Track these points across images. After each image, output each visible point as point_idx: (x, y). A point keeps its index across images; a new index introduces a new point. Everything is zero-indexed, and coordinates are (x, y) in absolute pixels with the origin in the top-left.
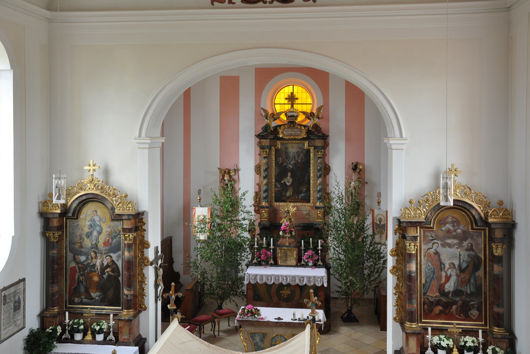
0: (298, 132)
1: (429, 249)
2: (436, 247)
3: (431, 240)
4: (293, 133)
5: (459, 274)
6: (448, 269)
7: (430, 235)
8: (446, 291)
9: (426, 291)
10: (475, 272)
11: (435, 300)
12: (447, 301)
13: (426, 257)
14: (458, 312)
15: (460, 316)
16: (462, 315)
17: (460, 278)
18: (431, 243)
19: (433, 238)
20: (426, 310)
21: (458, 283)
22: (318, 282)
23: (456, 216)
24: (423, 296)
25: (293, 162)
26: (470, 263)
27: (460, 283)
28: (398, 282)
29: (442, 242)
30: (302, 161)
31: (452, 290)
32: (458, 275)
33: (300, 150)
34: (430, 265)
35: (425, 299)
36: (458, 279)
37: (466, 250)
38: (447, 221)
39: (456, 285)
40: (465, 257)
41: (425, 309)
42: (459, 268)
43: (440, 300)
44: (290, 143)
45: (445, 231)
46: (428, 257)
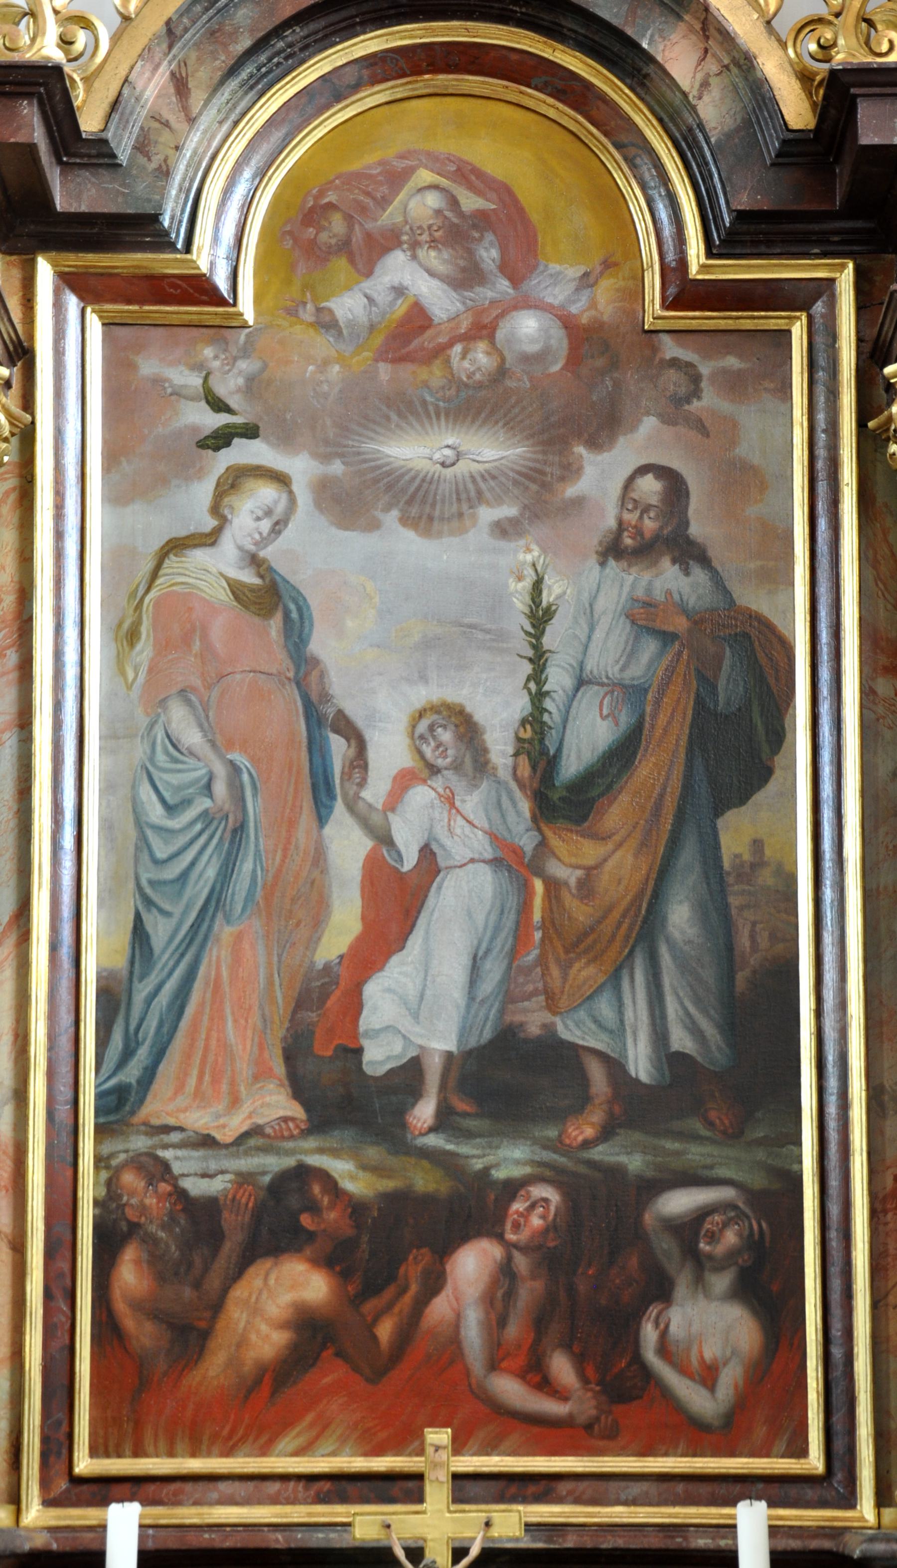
2: (266, 525)
3: (202, 444)
5: (527, 842)
9: (132, 1073)
10: (719, 810)
11: (244, 1179)
12: (388, 1185)
13: (144, 651)
14: (513, 1331)
17: (539, 886)
18: (200, 474)
19: (223, 419)
20: (129, 1322)
21: (514, 954)
24: (101, 1130)
26: (657, 703)
27: (541, 960)
29: (326, 458)
32: (517, 852)
34: (192, 737)
35: (129, 1178)
36: (512, 902)
38: (390, 216)
39: (488, 985)
40: (599, 635)
41: (120, 1306)
42: (525, 770)
45: (372, 328)
46: (163, 647)
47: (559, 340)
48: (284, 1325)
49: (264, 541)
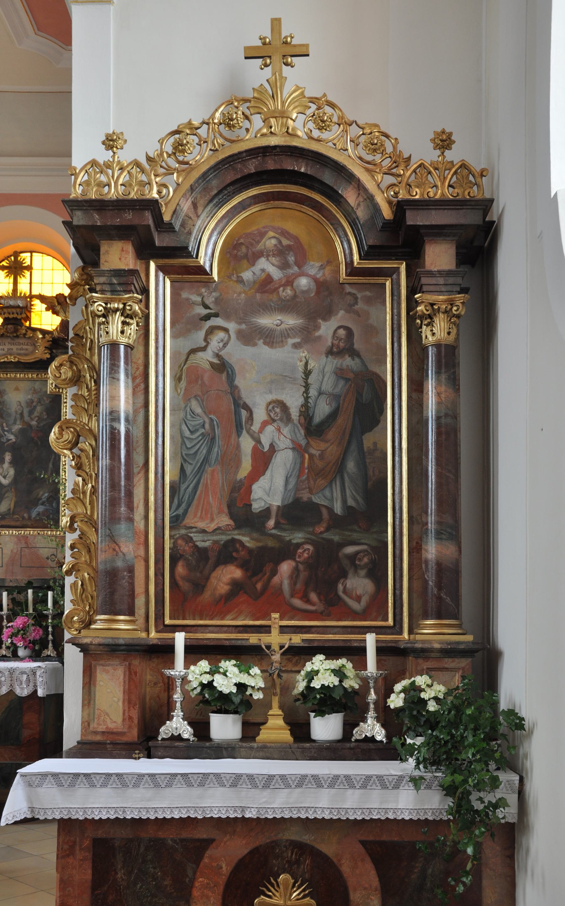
0: (27, 345)
1: (193, 351)
2: (221, 345)
4: (14, 348)
5: (303, 442)
6: (264, 424)
7: (199, 299)
8: (257, 506)
9: (180, 511)
10: (363, 433)
11: (215, 542)
12: (260, 544)
13: (183, 384)
14: (298, 586)
15: (308, 601)
16: (313, 596)
17: (307, 456)
18: (201, 329)
19: (208, 311)
21: (299, 476)
22: (21, 684)
23: (291, 227)
25: (17, 427)
26: (344, 400)
27: (308, 478)
28: (80, 479)
29: (240, 324)
30: (42, 425)
31: (276, 501)
32: (300, 446)
33: (35, 398)
34: (199, 410)
36: (298, 461)
37: (330, 352)
38: (260, 246)
39: (291, 486)
40: (326, 379)
42: (303, 421)
43: (233, 541)
44: (10, 379)
45: (254, 282)
46: (189, 382)
47: (313, 285)
48: (228, 584)
49: (221, 350)
